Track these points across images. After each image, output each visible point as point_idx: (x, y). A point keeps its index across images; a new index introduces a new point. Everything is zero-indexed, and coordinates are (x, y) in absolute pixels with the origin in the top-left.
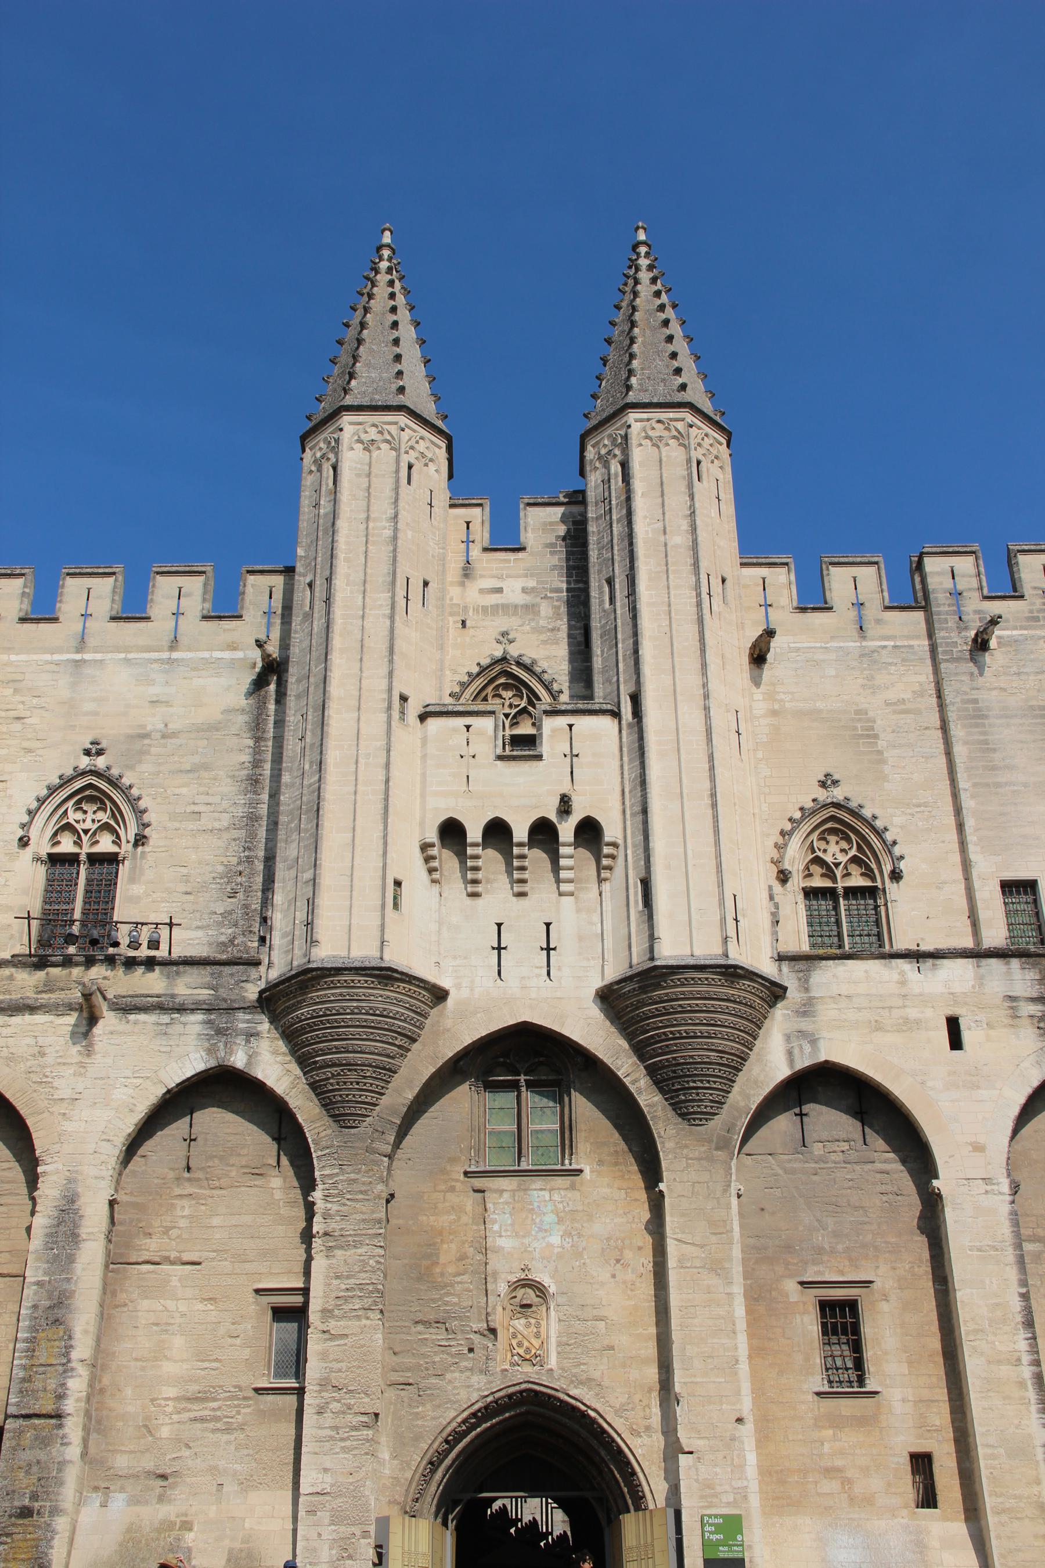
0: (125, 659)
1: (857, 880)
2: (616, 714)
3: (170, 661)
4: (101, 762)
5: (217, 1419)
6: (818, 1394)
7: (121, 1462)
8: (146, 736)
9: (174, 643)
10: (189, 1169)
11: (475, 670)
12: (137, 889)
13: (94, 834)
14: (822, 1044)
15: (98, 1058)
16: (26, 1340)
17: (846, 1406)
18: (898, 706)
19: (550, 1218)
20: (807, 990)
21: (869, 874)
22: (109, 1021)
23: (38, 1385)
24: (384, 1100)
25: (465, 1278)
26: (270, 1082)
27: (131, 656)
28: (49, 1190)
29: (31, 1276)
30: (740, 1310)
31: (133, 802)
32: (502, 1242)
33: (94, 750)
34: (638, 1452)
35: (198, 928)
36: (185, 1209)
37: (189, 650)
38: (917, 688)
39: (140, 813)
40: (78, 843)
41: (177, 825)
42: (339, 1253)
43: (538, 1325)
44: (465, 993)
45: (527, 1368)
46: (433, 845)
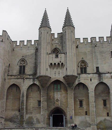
1: (85, 67)
2: (65, 54)
3: (29, 49)
4: (23, 58)
6: (79, 107)
7: (28, 112)
8: (27, 55)
12: (27, 68)
15: (25, 83)
17: (81, 108)
18: (89, 52)
19: (59, 94)
21: (86, 66)
22: (25, 80)
24: (47, 86)
28: (22, 93)
29: (21, 99)
30: (73, 101)
32: (56, 96)
36: (32, 94)
39: (27, 62)
40: (22, 65)
44: (52, 77)
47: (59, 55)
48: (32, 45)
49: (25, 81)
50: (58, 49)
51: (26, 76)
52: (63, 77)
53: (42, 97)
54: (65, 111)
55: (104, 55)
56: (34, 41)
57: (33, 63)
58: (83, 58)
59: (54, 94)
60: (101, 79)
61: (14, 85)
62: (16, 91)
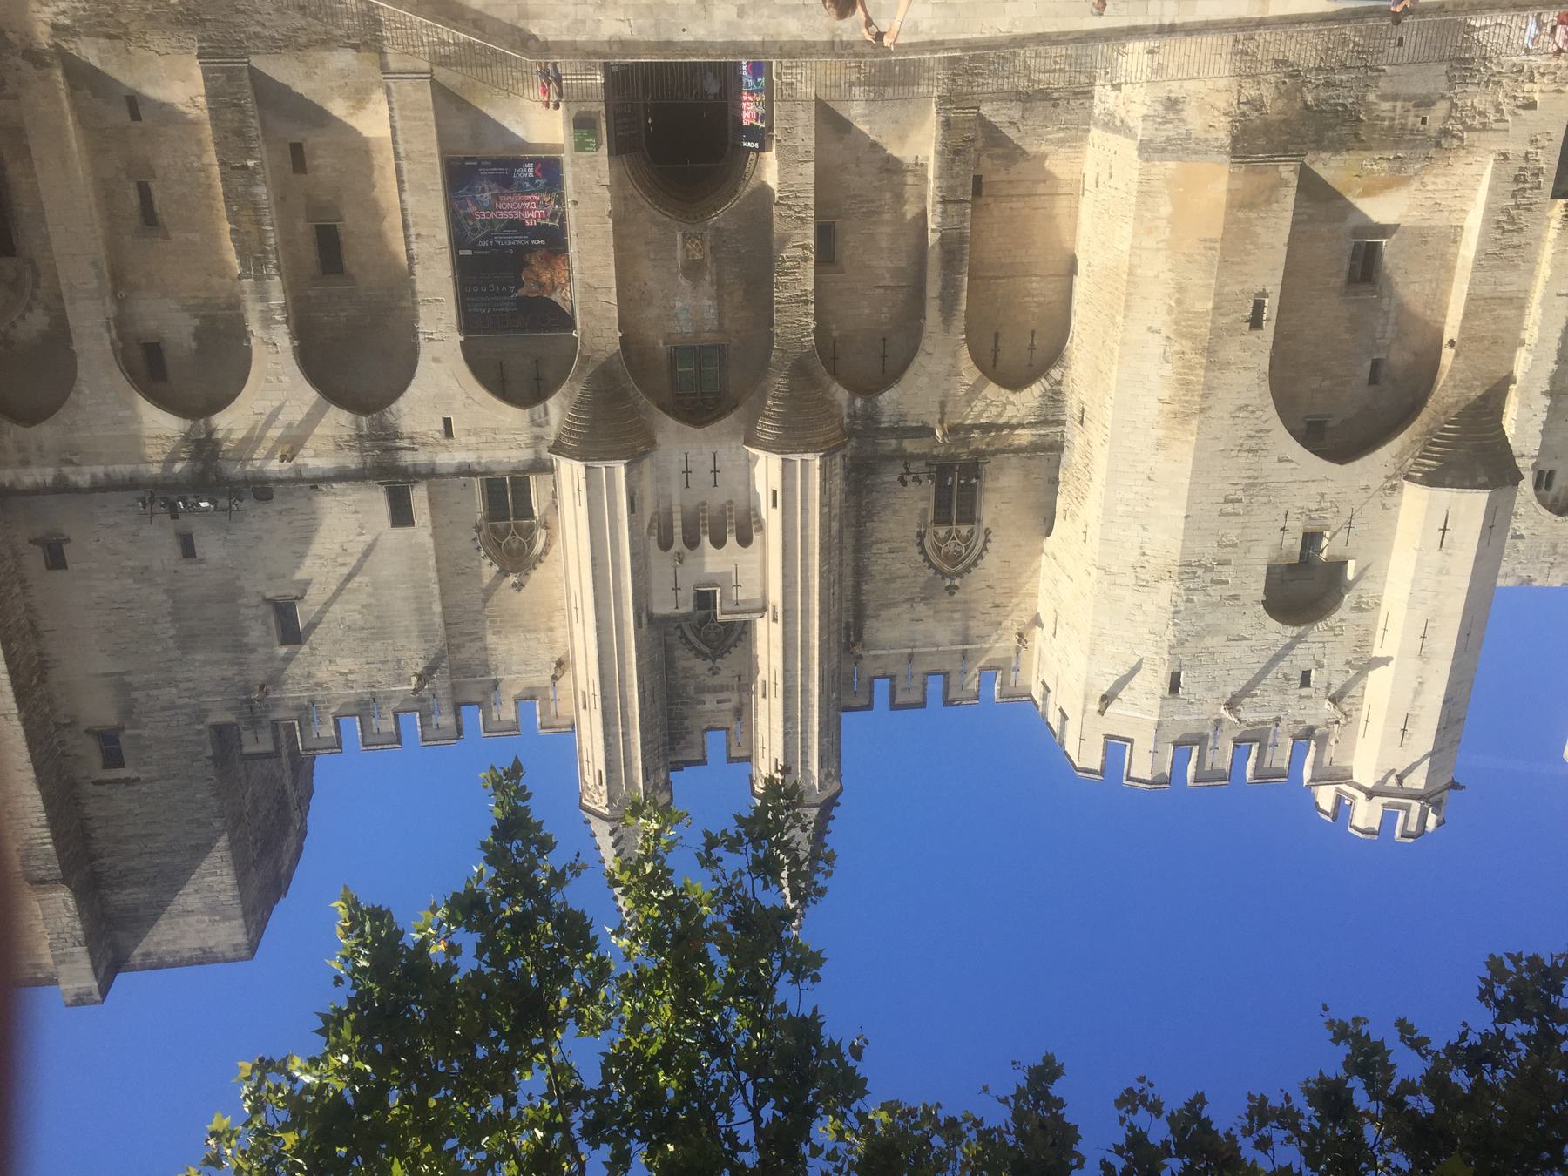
0: (939, 647)
1: (501, 524)
2: (651, 617)
4: (948, 582)
5: (861, 202)
8: (922, 599)
9: (911, 658)
10: (884, 340)
11: (732, 650)
12: (922, 505)
13: (949, 536)
14: (528, 419)
16: (966, 242)
19: (682, 317)
20: (536, 452)
23: (955, 218)
25: (728, 282)
26: (841, 389)
27: (935, 649)
28: (959, 323)
31: (927, 559)
32: (710, 302)
33: (951, 590)
34: (630, 186)
35: (886, 483)
37: (902, 655)
38: (462, 650)
39: (923, 552)
40: (958, 532)
41: (903, 545)
42: (799, 294)
43: (687, 256)
44: (734, 444)
45: (692, 231)
46: (756, 531)
47: (688, 607)
48: (884, 676)
49: (936, 408)
50: (700, 654)
51: (926, 450)
52: (652, 443)
53: (805, 293)
54: (630, 189)
55: (358, 616)
56: (871, 701)
57: (873, 543)
58: (519, 586)
59: (720, 315)
60: (373, 437)
61: (1015, 383)
62: (996, 335)
